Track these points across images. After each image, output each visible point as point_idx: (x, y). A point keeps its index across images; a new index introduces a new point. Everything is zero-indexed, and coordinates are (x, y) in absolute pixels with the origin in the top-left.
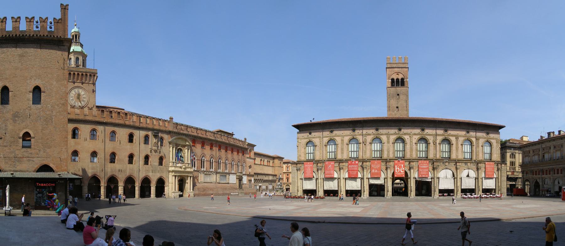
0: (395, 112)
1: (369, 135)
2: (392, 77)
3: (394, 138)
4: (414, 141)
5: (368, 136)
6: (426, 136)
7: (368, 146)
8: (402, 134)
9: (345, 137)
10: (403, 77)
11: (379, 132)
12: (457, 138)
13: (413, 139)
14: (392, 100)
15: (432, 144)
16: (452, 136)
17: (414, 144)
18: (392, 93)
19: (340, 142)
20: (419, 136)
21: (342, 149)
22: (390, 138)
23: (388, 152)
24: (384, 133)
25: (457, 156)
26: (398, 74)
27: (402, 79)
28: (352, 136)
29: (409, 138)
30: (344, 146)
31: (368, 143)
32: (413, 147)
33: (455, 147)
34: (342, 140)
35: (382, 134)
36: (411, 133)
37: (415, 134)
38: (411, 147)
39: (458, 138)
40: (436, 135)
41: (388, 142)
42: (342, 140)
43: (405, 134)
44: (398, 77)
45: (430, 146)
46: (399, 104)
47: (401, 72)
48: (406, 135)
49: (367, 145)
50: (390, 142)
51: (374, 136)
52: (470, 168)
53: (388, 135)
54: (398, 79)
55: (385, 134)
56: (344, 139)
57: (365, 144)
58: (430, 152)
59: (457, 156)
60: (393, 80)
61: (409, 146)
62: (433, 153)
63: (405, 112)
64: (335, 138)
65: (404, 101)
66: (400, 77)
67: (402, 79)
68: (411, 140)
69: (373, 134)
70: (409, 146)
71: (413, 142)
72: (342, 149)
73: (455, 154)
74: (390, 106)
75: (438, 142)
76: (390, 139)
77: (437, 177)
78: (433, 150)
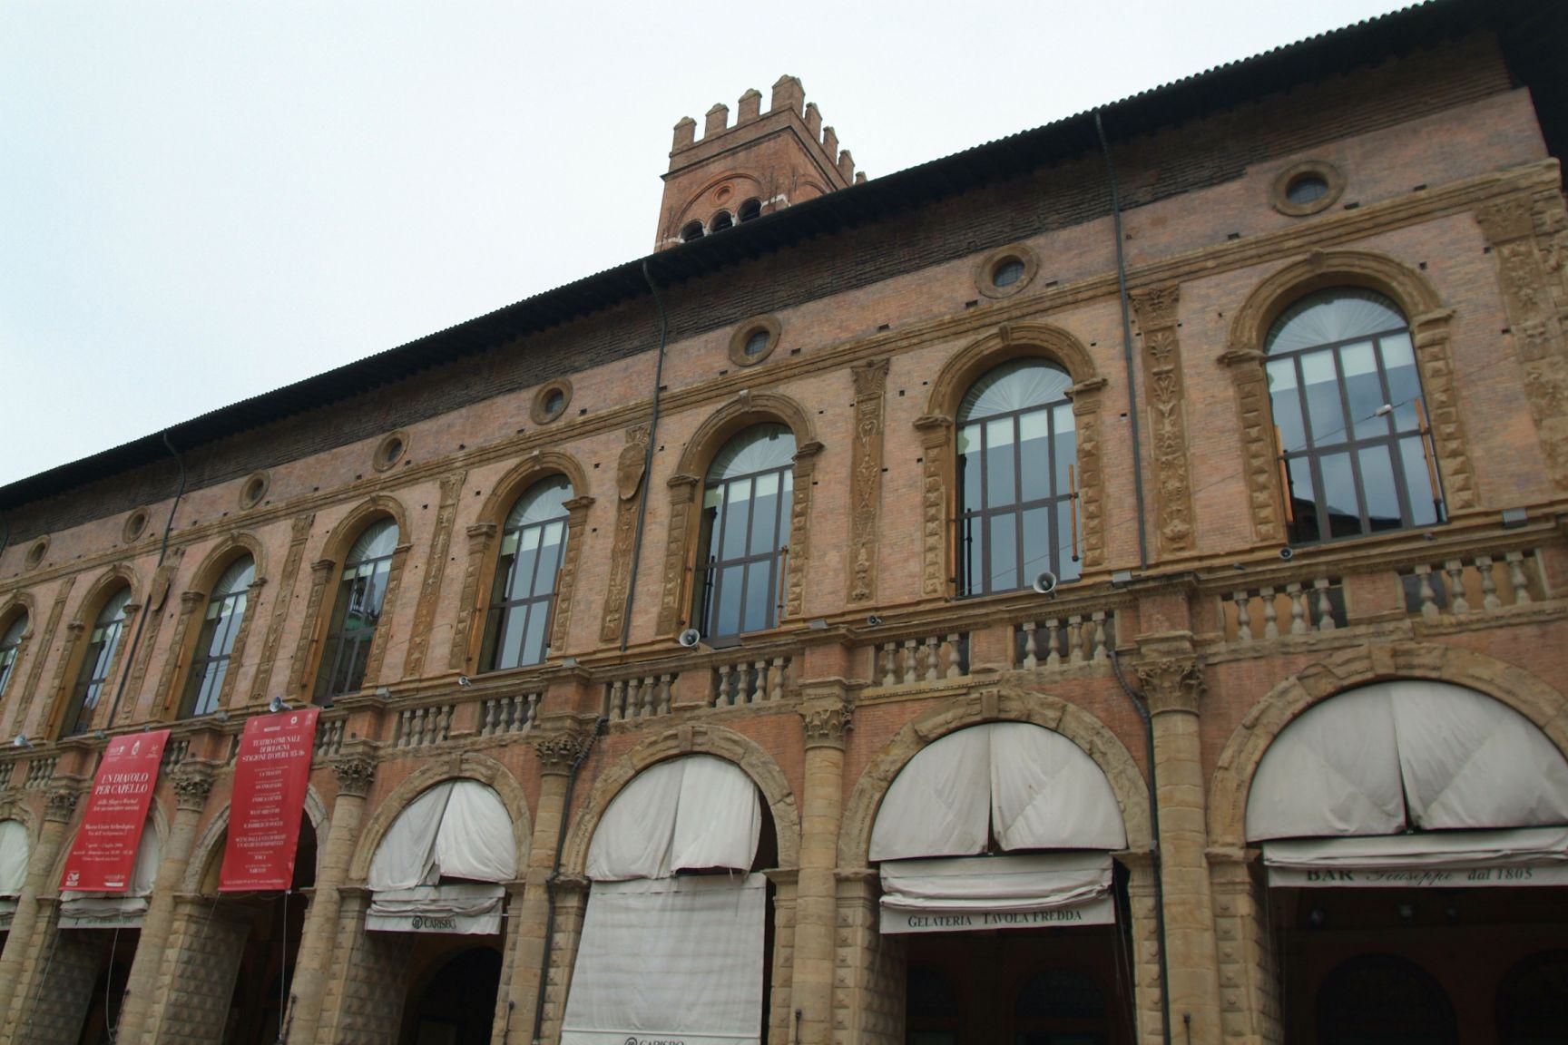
2: (688, 218)
11: (263, 502)
13: (467, 495)
15: (605, 512)
16: (818, 364)
20: (511, 463)
22: (313, 531)
23: (270, 653)
24: (282, 505)
26: (725, 191)
30: (54, 647)
33: (844, 472)
36: (461, 453)
37: (485, 456)
39: (885, 369)
40: (661, 404)
43: (414, 476)
44: (726, 206)
47: (741, 171)
52: (1014, 708)
59: (862, 578)
61: (421, 572)
62: (598, 601)
70: (422, 567)
73: (833, 558)
77: (570, 869)
78: (605, 568)
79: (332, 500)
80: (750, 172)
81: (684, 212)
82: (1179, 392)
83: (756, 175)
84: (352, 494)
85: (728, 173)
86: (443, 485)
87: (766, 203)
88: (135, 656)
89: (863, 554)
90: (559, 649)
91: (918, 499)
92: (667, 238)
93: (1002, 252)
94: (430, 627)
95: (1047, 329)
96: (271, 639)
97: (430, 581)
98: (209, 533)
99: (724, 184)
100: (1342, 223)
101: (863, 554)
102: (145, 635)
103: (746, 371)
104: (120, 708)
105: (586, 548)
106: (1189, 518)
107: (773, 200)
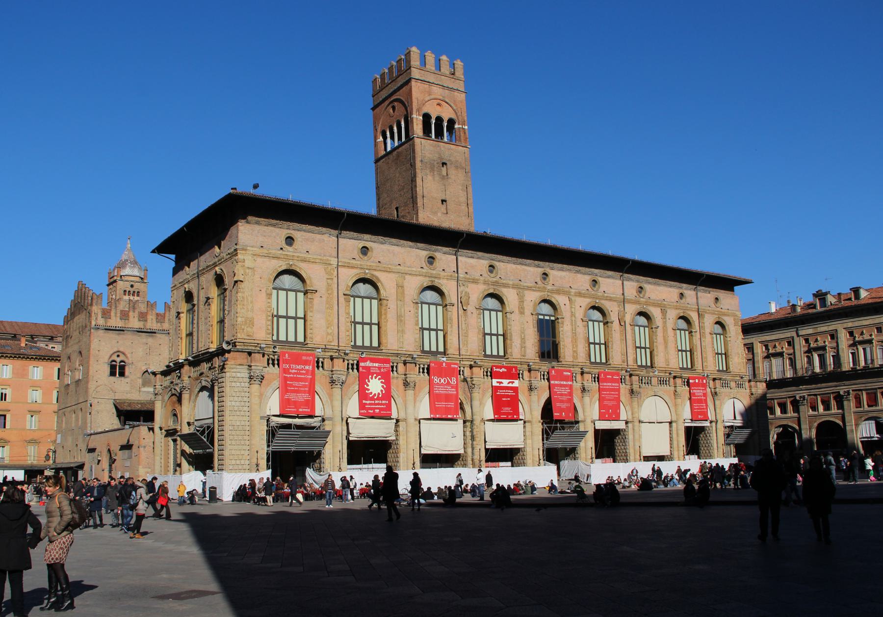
0: (439, 214)
1: (475, 281)
3: (533, 299)
4: (579, 314)
5: (472, 286)
6: (603, 302)
7: (473, 319)
8: (552, 291)
9: (407, 277)
10: (453, 116)
11: (498, 277)
12: (664, 312)
14: (430, 178)
15: (616, 325)
17: (580, 323)
18: (428, 155)
19: (394, 291)
21: (400, 319)
22: (525, 298)
23: (523, 340)
24: (511, 283)
25: (667, 361)
26: (439, 104)
27: (451, 122)
28: (427, 279)
29: (567, 302)
31: (470, 308)
32: (578, 330)
34: (400, 287)
35: (506, 286)
37: (580, 294)
38: (573, 330)
41: (522, 312)
42: (400, 287)
43: (559, 292)
45: (613, 331)
46: (448, 192)
48: (559, 294)
49: (469, 312)
50: (526, 311)
51: (485, 287)
53: (518, 287)
54: (439, 120)
55: (514, 287)
56: (406, 284)
57: (465, 308)
58: (615, 347)
60: (427, 117)
63: (463, 218)
64: (376, 273)
65: (461, 187)
66: (447, 114)
67: (451, 122)
68: (573, 310)
69: (485, 283)
71: (577, 315)
72: (400, 319)
74: (425, 194)
75: (628, 319)
76: (525, 303)
78: (619, 342)
79: (529, 288)
80: (452, 105)
81: (424, 104)
82: (705, 337)
83: (455, 108)
84: (537, 289)
85: (441, 98)
86: (570, 300)
87: (461, 126)
88: (460, 326)
89: (667, 356)
90: (613, 362)
91: (674, 346)
92: (419, 115)
93: (681, 291)
94: (577, 346)
95: (689, 315)
96: (523, 336)
97: (574, 331)
98: (479, 282)
99: (441, 102)
100: (721, 312)
101: (667, 356)
102: (462, 319)
103: (642, 299)
104: (461, 347)
105: (613, 335)
106: (707, 363)
107: (464, 127)
